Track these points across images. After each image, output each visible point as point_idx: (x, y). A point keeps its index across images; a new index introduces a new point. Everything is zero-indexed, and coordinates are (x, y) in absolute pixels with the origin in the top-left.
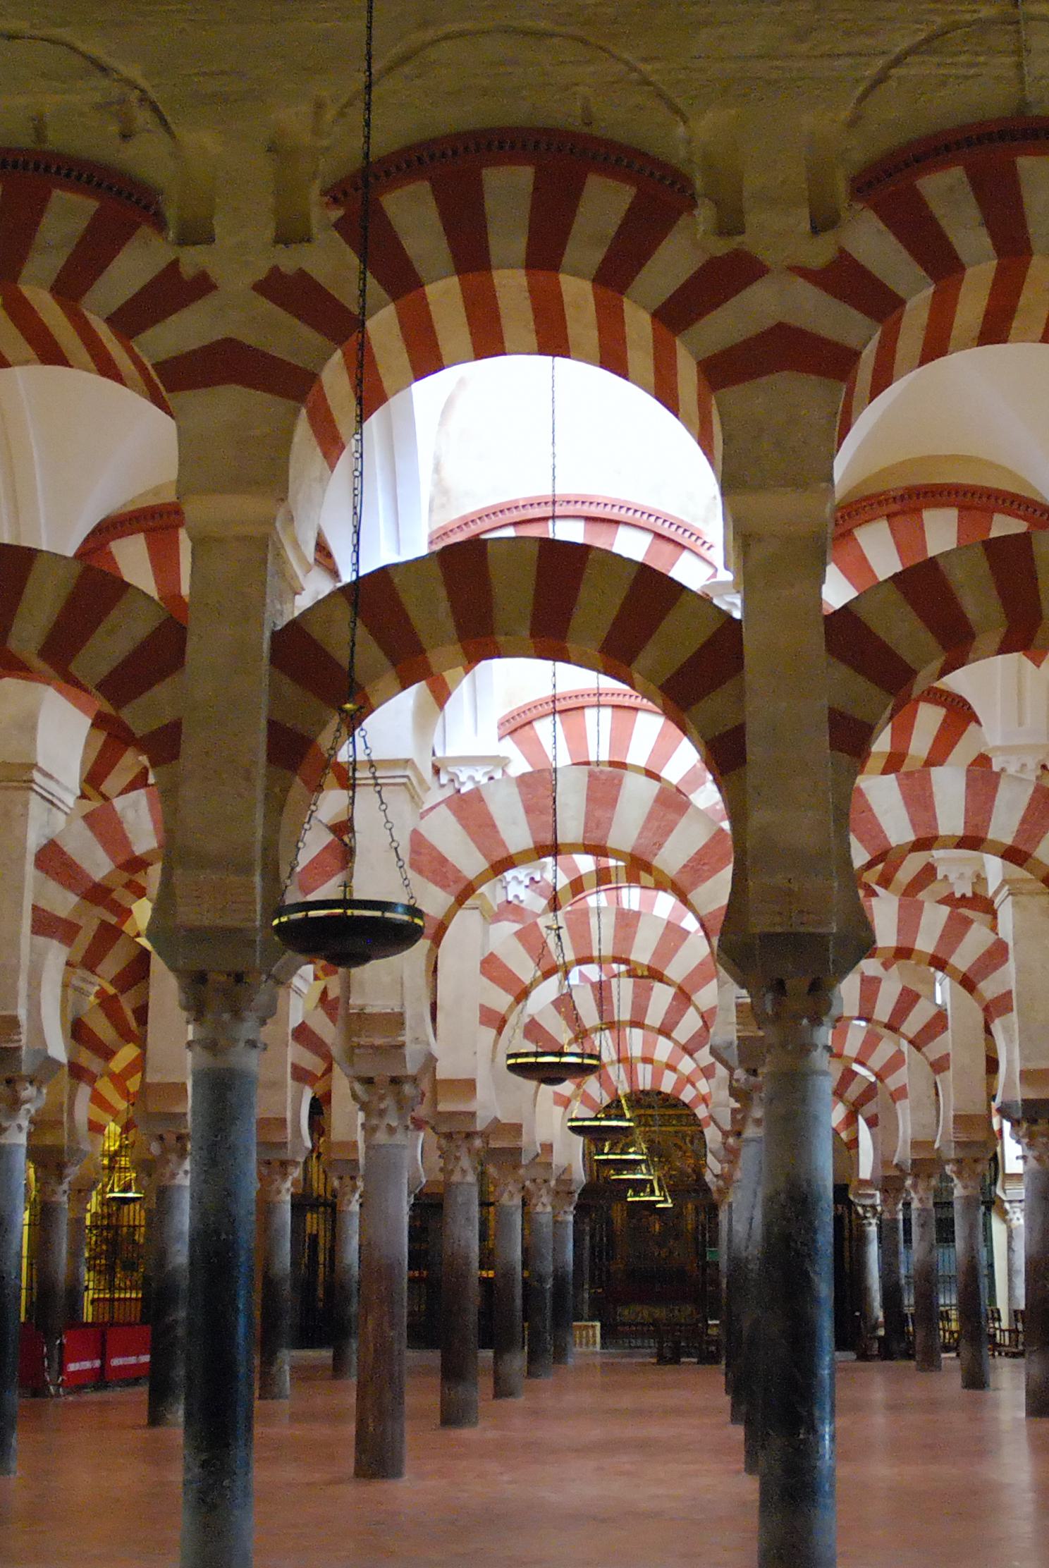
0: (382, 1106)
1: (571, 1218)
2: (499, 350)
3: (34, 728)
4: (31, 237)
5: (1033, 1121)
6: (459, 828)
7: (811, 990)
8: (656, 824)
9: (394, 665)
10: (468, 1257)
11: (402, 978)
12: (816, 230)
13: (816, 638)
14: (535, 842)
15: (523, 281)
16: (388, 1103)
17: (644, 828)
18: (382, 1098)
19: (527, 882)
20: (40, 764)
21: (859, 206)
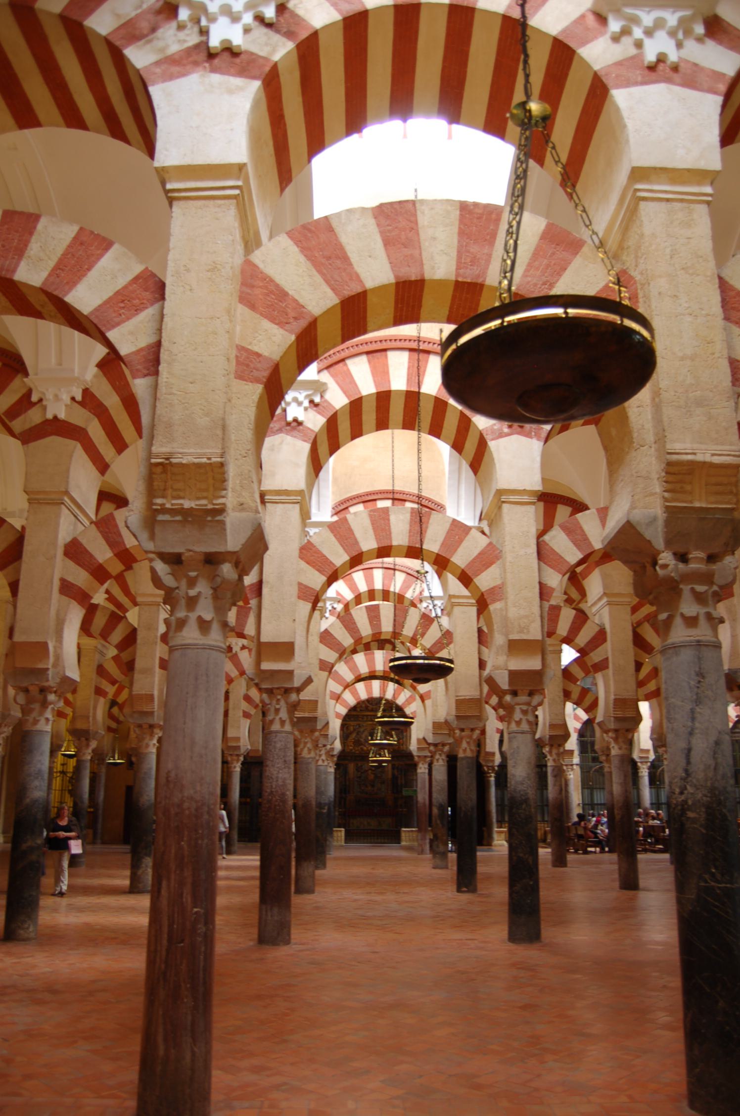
0: (192, 593)
1: (332, 770)
6: (302, 258)
8: (545, 262)
10: (284, 794)
11: (223, 419)
14: (396, 277)
16: (202, 588)
18: (192, 583)
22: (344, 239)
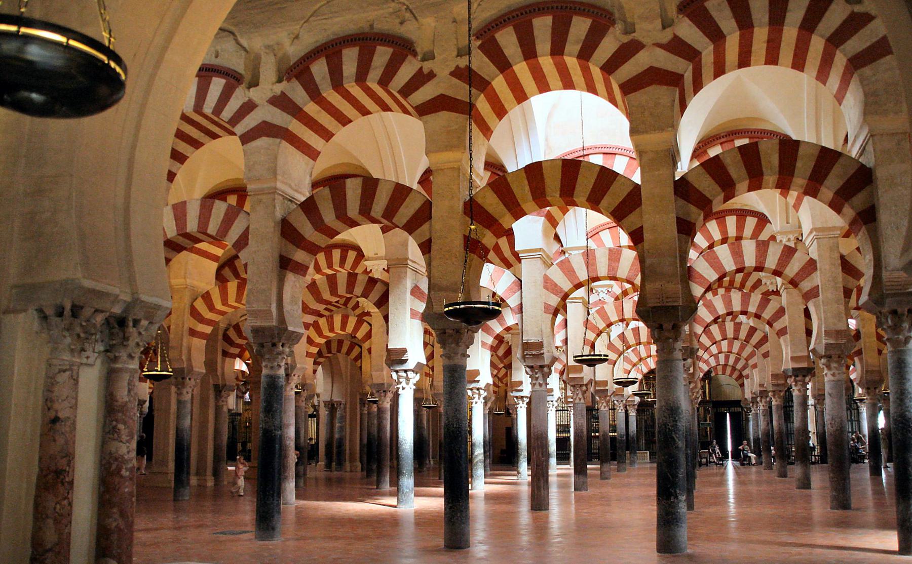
0: (537, 376)
2: (549, 90)
3: (407, 245)
4: (370, 65)
5: (797, 376)
7: (673, 328)
9: (509, 212)
12: (664, 27)
13: (670, 190)
15: (551, 60)
17: (630, 269)
18: (536, 373)
19: (606, 292)
20: (410, 258)
21: (681, 16)
22: (573, 265)
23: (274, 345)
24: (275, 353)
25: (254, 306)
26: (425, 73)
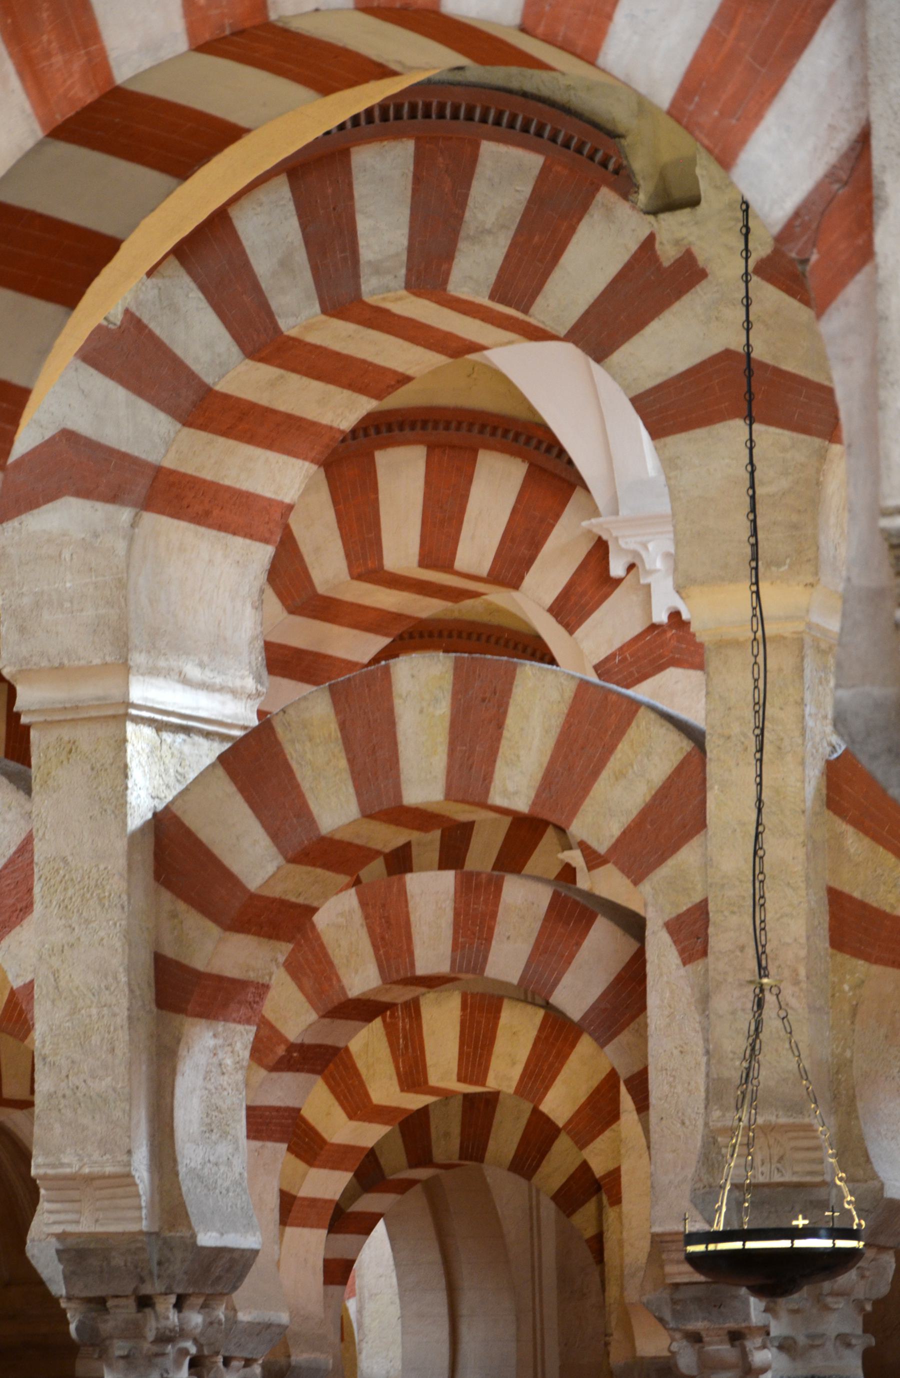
23: (145, 1302)
24: (151, 1335)
25: (65, 1160)
26: (666, 264)
